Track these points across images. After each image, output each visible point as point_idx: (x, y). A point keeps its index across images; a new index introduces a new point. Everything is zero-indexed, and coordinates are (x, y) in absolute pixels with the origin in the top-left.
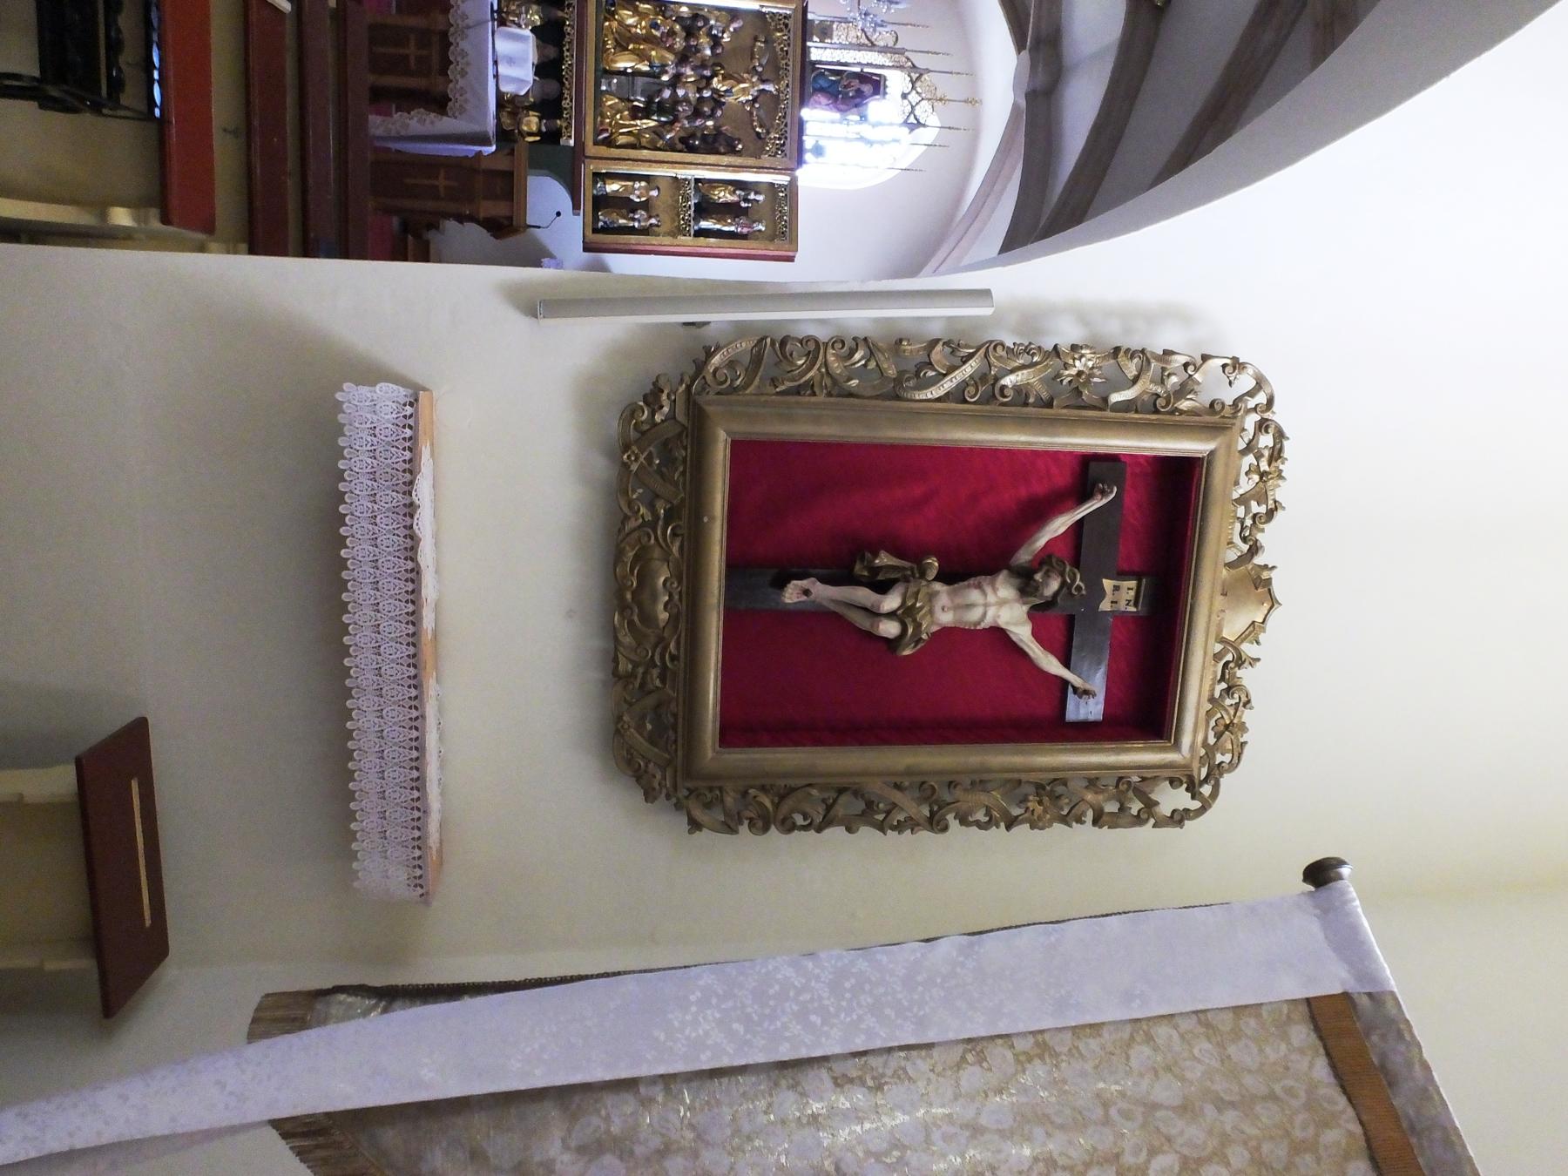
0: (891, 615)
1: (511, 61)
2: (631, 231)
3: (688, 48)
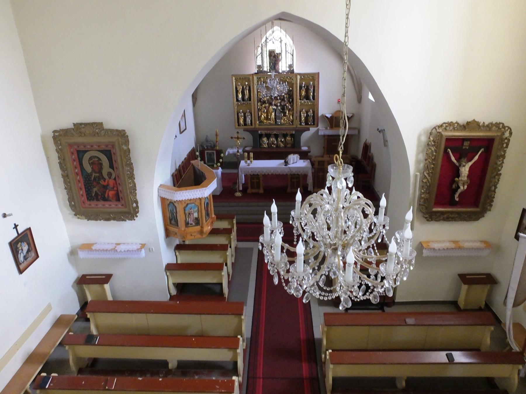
0: (464, 187)
1: (294, 160)
2: (314, 116)
3: (268, 103)
